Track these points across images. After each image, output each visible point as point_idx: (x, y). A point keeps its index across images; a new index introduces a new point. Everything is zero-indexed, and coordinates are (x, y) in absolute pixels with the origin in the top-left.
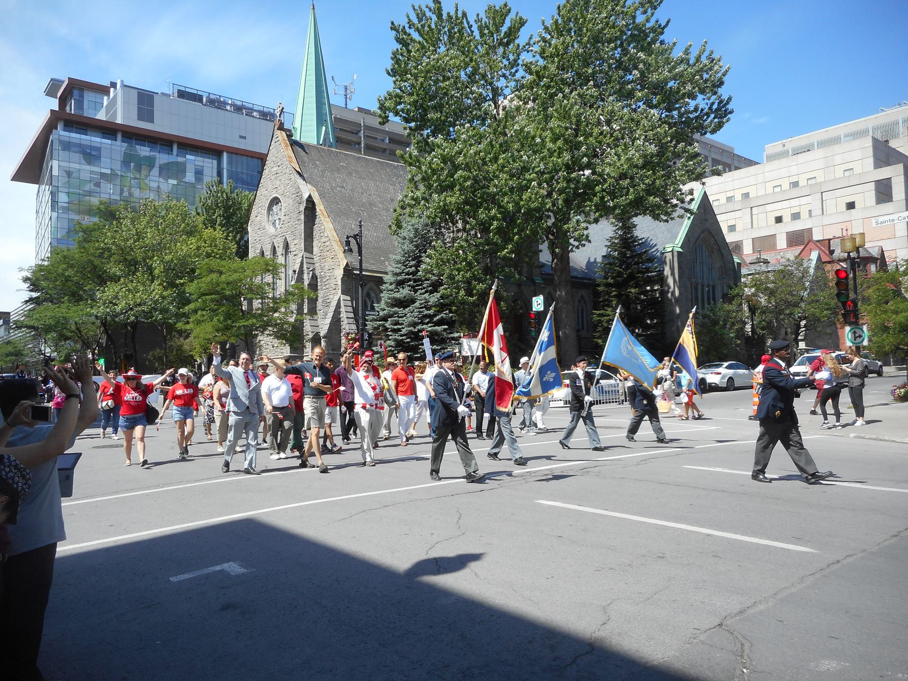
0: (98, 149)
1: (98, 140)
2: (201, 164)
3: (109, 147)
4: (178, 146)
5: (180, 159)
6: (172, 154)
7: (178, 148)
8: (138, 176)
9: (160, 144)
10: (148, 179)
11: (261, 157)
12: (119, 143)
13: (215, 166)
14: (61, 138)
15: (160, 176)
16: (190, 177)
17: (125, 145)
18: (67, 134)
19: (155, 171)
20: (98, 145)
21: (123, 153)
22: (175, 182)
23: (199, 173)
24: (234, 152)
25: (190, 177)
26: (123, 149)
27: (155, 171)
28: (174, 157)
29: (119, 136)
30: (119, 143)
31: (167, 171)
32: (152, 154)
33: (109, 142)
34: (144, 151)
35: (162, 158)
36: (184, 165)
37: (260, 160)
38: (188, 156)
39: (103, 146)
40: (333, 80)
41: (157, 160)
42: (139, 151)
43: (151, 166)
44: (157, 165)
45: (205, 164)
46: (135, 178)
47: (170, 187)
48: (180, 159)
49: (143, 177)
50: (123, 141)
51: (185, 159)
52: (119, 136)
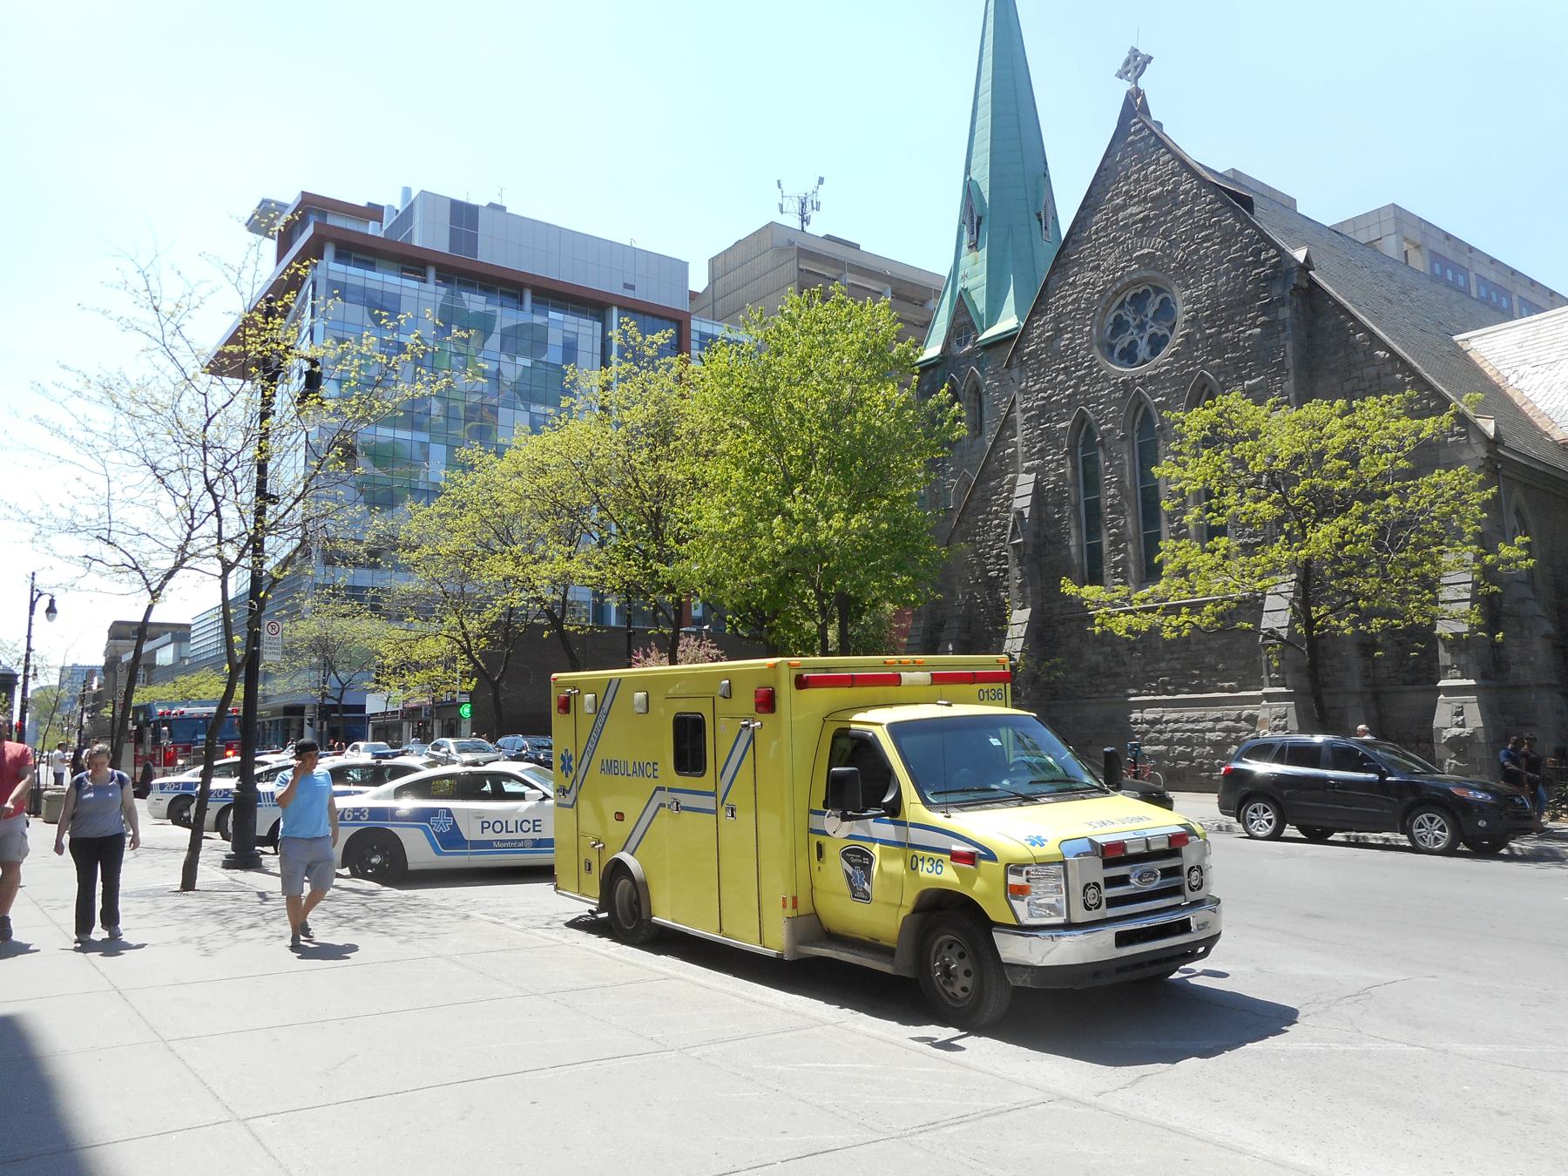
0: (397, 299)
1: (396, 280)
2: (573, 328)
3: (415, 294)
4: (533, 294)
5: (538, 319)
6: (521, 310)
7: (533, 301)
8: (463, 350)
9: (502, 293)
10: (481, 355)
11: (679, 318)
12: (431, 287)
13: (599, 333)
14: (333, 276)
15: (502, 349)
16: (554, 355)
17: (443, 290)
18: (341, 267)
19: (494, 342)
20: (396, 290)
21: (438, 306)
22: (527, 362)
23: (570, 350)
24: (633, 308)
25: (554, 355)
26: (440, 298)
27: (494, 342)
28: (526, 315)
29: (431, 273)
30: (431, 287)
31: (514, 340)
32: (490, 308)
33: (415, 284)
34: (475, 302)
35: (506, 317)
36: (544, 329)
37: (675, 325)
38: (552, 315)
39: (405, 291)
40: (779, 187)
41: (498, 319)
42: (467, 303)
43: (487, 332)
44: (497, 329)
45: (582, 330)
46: (459, 354)
47: (519, 371)
48: (538, 319)
49: (472, 351)
50: (437, 284)
51: (546, 320)
52: (431, 273)
